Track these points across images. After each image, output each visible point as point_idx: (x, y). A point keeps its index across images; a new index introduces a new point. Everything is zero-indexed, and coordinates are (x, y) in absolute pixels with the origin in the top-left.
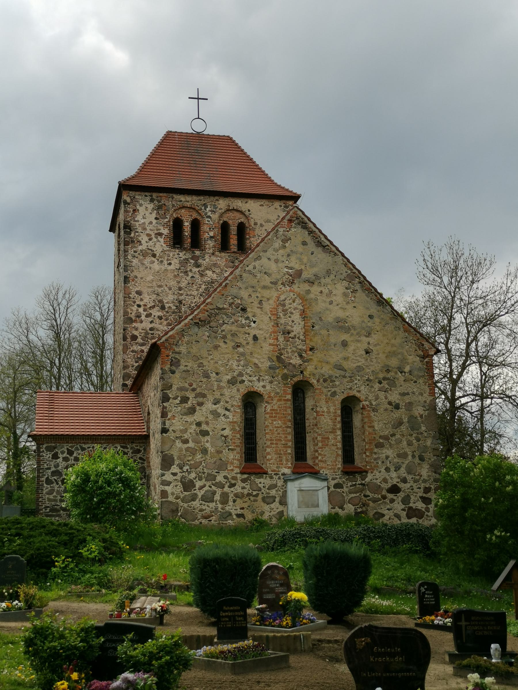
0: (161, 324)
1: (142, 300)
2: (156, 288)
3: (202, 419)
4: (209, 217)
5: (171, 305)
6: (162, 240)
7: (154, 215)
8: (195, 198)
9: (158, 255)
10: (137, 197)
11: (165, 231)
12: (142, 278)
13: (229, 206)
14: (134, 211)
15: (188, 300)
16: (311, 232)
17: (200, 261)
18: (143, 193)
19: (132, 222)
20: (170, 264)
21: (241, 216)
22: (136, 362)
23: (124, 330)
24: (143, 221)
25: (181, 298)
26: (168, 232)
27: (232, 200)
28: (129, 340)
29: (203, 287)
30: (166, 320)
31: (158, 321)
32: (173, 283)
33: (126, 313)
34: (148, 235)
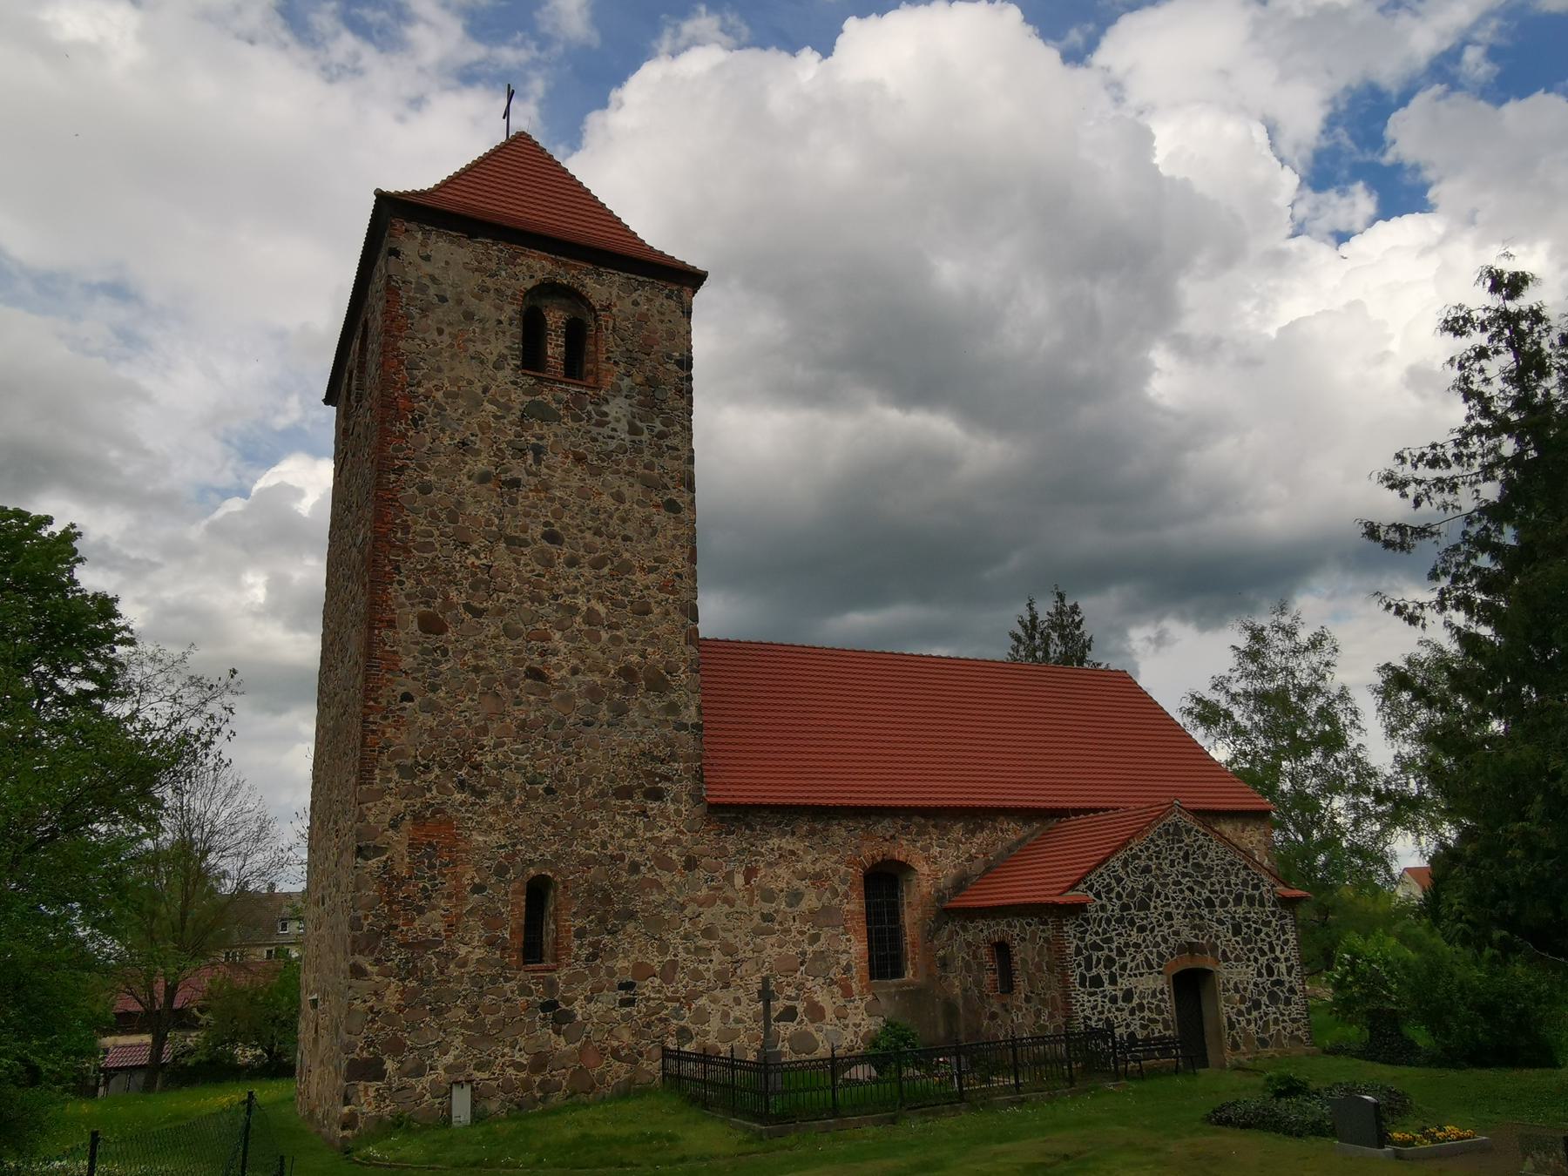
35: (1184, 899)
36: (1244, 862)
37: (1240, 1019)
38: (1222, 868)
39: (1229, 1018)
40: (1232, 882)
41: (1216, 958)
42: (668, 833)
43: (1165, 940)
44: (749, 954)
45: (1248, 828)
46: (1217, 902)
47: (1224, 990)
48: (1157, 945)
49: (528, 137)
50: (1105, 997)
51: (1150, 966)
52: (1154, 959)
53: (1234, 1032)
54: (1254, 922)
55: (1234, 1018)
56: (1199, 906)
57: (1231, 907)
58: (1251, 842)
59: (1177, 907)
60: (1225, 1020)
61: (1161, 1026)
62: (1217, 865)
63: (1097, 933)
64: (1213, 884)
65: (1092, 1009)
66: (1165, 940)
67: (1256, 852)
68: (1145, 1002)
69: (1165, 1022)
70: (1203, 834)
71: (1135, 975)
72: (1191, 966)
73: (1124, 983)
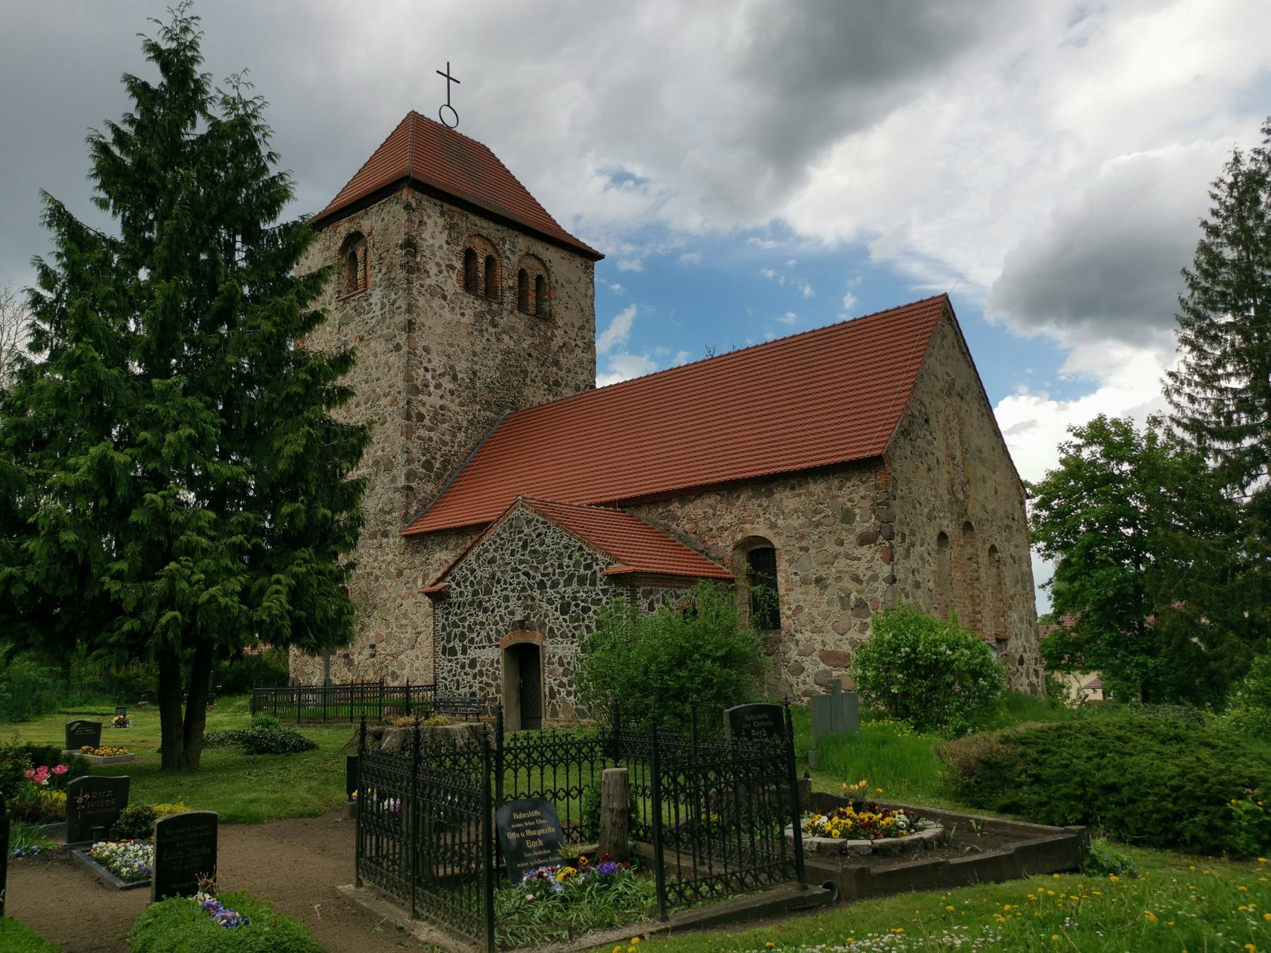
0: (452, 401)
1: (430, 361)
2: (447, 348)
3: (915, 566)
4: (507, 258)
5: (464, 376)
6: (454, 276)
7: (445, 236)
8: (492, 225)
9: (449, 298)
10: (424, 202)
11: (459, 265)
12: (430, 328)
13: (529, 248)
14: (420, 222)
15: (483, 373)
16: (956, 333)
17: (497, 318)
18: (431, 199)
19: (418, 239)
20: (463, 315)
21: (540, 267)
22: (424, 455)
23: (408, 403)
24: (431, 241)
25: (476, 367)
26: (462, 266)
27: (533, 241)
28: (414, 419)
29: (500, 357)
30: (459, 396)
31: (448, 396)
32: (465, 344)
33: (408, 378)
34: (438, 265)
35: (519, 583)
36: (579, 544)
37: (561, 690)
38: (557, 552)
39: (551, 689)
40: (565, 564)
41: (544, 634)
42: (390, 557)
43: (502, 619)
44: (423, 629)
45: (849, 484)
46: (549, 584)
47: (548, 663)
48: (496, 623)
49: (416, 113)
50: (457, 663)
51: (490, 641)
52: (493, 635)
53: (554, 701)
54: (582, 601)
55: (556, 688)
56: (532, 588)
57: (561, 588)
58: (851, 500)
59: (513, 591)
60: (547, 690)
61: (493, 690)
62: (552, 550)
63: (456, 614)
64: (546, 568)
65: (449, 672)
66: (502, 619)
67: (857, 511)
68: (484, 669)
69: (498, 687)
70: (542, 523)
71: (479, 648)
72: (521, 640)
73: (472, 653)
